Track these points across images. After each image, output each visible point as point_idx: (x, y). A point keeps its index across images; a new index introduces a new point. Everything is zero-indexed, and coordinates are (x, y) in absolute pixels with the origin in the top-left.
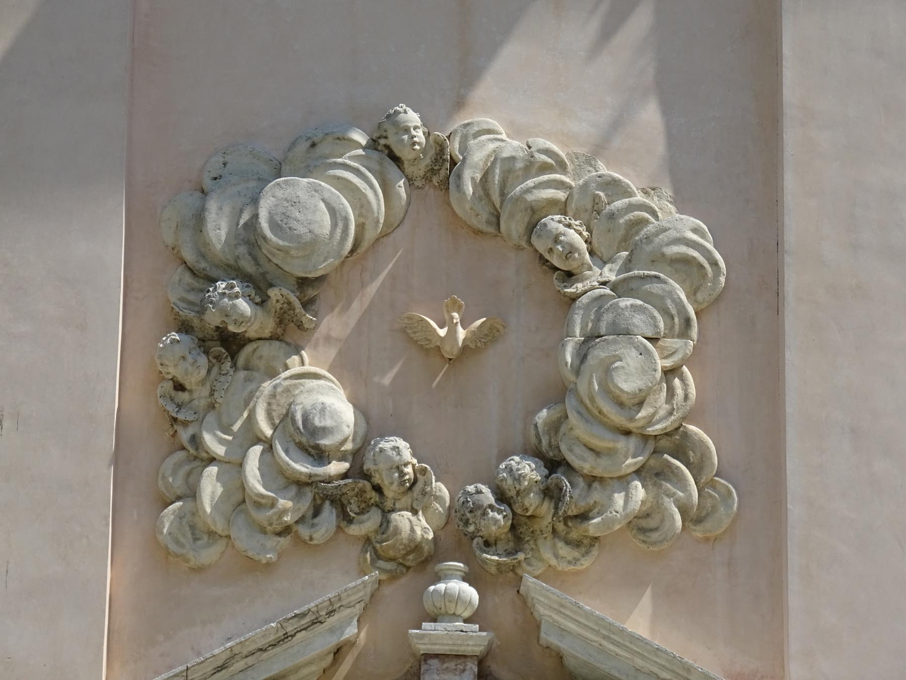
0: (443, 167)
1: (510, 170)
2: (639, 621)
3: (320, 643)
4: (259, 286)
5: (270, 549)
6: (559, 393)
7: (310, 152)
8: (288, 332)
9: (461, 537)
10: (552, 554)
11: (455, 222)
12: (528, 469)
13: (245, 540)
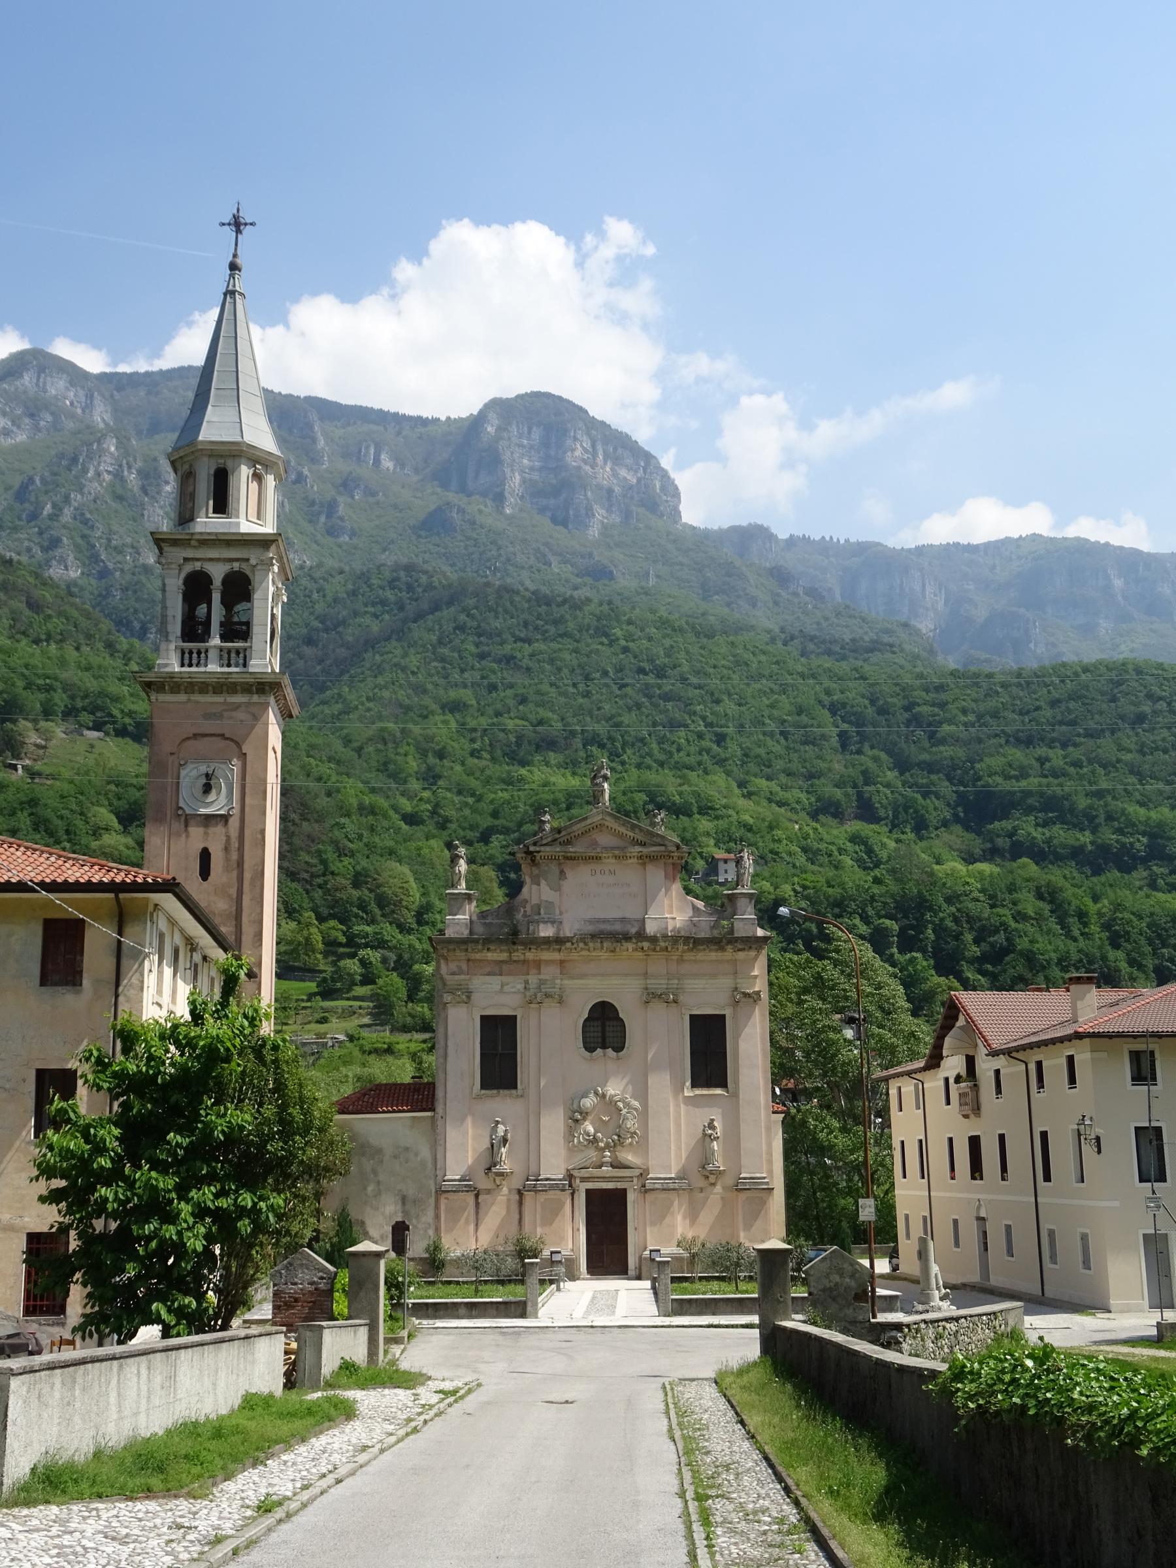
0: (604, 1096)
1: (612, 1096)
2: (630, 1158)
4: (581, 1113)
6: (620, 1127)
7: (584, 1095)
8: (584, 1119)
9: (607, 1146)
10: (619, 1148)
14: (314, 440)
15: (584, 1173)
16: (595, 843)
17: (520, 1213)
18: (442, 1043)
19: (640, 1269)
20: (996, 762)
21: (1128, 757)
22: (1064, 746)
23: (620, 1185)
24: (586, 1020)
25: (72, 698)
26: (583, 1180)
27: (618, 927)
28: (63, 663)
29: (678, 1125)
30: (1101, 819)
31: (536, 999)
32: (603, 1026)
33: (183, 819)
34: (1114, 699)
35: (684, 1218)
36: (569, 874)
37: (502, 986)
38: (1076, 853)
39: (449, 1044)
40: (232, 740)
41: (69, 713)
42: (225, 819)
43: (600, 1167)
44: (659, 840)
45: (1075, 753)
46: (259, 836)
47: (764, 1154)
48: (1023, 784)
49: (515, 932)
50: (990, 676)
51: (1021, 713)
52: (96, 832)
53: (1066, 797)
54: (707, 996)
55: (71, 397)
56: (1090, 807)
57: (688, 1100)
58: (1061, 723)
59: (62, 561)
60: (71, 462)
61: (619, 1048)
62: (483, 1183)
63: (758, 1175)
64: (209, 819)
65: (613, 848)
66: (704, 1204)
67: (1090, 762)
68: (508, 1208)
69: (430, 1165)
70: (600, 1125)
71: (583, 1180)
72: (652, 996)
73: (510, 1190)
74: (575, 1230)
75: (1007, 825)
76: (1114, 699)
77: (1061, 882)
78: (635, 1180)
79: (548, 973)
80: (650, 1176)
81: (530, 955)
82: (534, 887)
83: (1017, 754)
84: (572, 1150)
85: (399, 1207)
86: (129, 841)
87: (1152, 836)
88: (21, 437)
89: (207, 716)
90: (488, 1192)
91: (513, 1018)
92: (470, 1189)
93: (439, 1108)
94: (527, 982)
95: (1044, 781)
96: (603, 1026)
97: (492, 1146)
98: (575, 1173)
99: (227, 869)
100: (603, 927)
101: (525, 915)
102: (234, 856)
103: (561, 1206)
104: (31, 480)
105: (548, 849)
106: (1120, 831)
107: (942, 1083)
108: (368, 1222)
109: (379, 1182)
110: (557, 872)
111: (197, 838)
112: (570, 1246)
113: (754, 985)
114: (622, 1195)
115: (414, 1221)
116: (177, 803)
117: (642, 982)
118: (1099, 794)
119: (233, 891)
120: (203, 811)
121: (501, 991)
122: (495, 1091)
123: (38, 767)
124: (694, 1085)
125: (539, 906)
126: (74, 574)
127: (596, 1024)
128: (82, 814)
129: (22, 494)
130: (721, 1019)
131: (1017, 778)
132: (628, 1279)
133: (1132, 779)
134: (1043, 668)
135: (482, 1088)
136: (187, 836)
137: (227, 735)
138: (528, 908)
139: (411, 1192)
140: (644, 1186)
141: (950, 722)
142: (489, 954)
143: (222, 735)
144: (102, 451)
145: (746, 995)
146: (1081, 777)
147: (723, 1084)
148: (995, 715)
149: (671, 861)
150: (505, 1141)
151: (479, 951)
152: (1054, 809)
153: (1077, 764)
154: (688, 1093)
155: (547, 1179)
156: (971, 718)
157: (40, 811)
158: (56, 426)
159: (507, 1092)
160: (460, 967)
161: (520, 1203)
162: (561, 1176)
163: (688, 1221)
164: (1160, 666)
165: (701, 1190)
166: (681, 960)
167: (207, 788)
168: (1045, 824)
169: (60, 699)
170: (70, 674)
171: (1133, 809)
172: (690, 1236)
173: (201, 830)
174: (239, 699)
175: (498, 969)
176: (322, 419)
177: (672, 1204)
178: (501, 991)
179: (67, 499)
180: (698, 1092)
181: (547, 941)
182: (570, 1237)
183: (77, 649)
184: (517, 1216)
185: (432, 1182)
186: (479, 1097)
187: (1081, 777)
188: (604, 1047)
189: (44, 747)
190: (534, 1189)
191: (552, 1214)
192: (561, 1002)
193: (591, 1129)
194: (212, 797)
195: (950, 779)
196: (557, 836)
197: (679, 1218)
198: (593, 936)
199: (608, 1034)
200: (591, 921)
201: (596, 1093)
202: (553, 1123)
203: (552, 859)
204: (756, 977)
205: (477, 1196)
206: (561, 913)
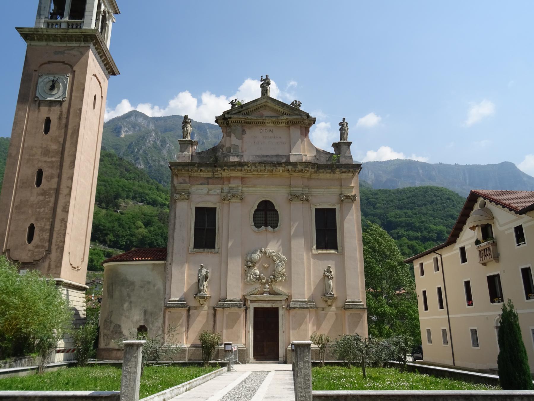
0: (265, 253)
1: (271, 253)
2: (280, 289)
3: (257, 290)
4: (252, 263)
5: (253, 283)
6: (274, 271)
7: (255, 252)
8: (254, 266)
9: (267, 282)
10: (274, 283)
11: (266, 257)
12: (272, 277)
13: (251, 283)
14: (207, 134)
15: (253, 298)
16: (262, 116)
17: (214, 322)
18: (173, 221)
19: (286, 357)
20: (393, 214)
21: (430, 212)
22: (411, 209)
23: (274, 306)
24: (256, 211)
25: (136, 194)
26: (252, 302)
27: (274, 159)
28: (134, 185)
29: (309, 270)
30: (423, 229)
31: (227, 198)
32: (266, 214)
33: (37, 103)
34: (425, 197)
35: (313, 325)
36: (248, 131)
37: (208, 191)
38: (416, 238)
39: (177, 222)
40: (69, 65)
41: (134, 198)
42: (60, 103)
43: (263, 294)
44: (297, 112)
45: (415, 211)
46: (78, 112)
47: (357, 291)
48: (400, 219)
49: (216, 159)
50: (390, 191)
51: (399, 200)
52: (137, 228)
53: (413, 223)
54: (325, 199)
55: (144, 122)
56: (420, 226)
57: (315, 256)
58: (410, 203)
59: (139, 163)
60: (142, 138)
61: (275, 226)
62: (193, 303)
63: (357, 300)
64: (52, 103)
65: (272, 117)
66: (325, 317)
67: (419, 213)
68: (208, 317)
69: (162, 292)
70: (263, 269)
71: (252, 302)
72: (293, 197)
73: (209, 308)
74: (247, 332)
75: (396, 231)
76: (425, 197)
77: (415, 244)
78: (283, 302)
79: (234, 184)
80: (293, 300)
81: (224, 174)
82: (228, 138)
83: (398, 212)
84: (246, 284)
85: (142, 317)
86: (146, 230)
87: (438, 234)
88: (131, 133)
89: (56, 53)
90: (196, 308)
91: (215, 209)
92: (183, 306)
93: (169, 258)
94: (222, 189)
95: (407, 219)
96: (266, 214)
97: (199, 281)
98: (248, 298)
99: (59, 128)
100: (266, 159)
101: (222, 153)
102: (64, 122)
103: (239, 317)
104: (132, 143)
105: (235, 116)
106: (429, 232)
107: (458, 251)
108: (123, 326)
109: (131, 302)
110: (241, 130)
111: (44, 113)
112: (243, 341)
113: (352, 192)
114: (275, 311)
115: (151, 325)
116: (35, 94)
117: (288, 189)
118: (422, 222)
119: (61, 140)
120: (49, 98)
121: (208, 194)
122: (202, 250)
123: (124, 212)
124: (318, 248)
125: (230, 148)
126: (142, 167)
127: (261, 213)
128: (134, 223)
129: (129, 146)
130: (333, 211)
131: (398, 218)
132: (279, 363)
133: (431, 218)
134: (404, 188)
135: (195, 247)
136: (39, 111)
137: (66, 62)
138: (224, 149)
139: (150, 308)
140: (289, 306)
141: (379, 203)
142: (202, 173)
143: (63, 62)
144: (151, 135)
145: (347, 197)
146: (417, 217)
147: (335, 247)
148: (392, 201)
149: (304, 125)
150: (206, 278)
151: (196, 171)
152: (410, 226)
153: (415, 214)
154: (315, 252)
155: (231, 301)
156: (385, 202)
157: (121, 222)
158: (140, 130)
159: (209, 250)
160: (184, 180)
161: (215, 315)
162: (239, 299)
163: (315, 328)
164: (438, 188)
165: (323, 309)
166: (310, 178)
167: (52, 88)
168: (407, 230)
169: (131, 194)
170: (135, 188)
171: (432, 226)
172: (318, 334)
173: (47, 108)
174: (74, 44)
175: (207, 181)
176: (209, 128)
177: (306, 317)
178: (208, 194)
179: (141, 148)
180: (320, 251)
181: (234, 164)
182: (244, 337)
183: (138, 182)
184: (212, 323)
185: (162, 302)
186: (192, 253)
187: (417, 217)
188: (266, 225)
189: (126, 207)
190: (223, 307)
191: (233, 322)
192: (241, 199)
193: (258, 272)
194: (54, 92)
195: (379, 218)
196: (240, 109)
197: (310, 325)
198: (260, 163)
199: (268, 219)
200: (259, 156)
201: (261, 251)
202: (235, 267)
203: (238, 123)
204: (353, 187)
205: (189, 311)
206: (242, 152)
